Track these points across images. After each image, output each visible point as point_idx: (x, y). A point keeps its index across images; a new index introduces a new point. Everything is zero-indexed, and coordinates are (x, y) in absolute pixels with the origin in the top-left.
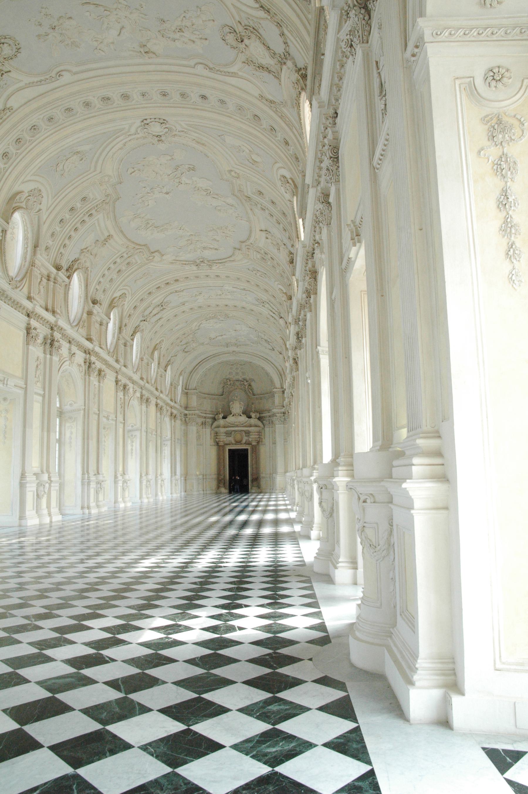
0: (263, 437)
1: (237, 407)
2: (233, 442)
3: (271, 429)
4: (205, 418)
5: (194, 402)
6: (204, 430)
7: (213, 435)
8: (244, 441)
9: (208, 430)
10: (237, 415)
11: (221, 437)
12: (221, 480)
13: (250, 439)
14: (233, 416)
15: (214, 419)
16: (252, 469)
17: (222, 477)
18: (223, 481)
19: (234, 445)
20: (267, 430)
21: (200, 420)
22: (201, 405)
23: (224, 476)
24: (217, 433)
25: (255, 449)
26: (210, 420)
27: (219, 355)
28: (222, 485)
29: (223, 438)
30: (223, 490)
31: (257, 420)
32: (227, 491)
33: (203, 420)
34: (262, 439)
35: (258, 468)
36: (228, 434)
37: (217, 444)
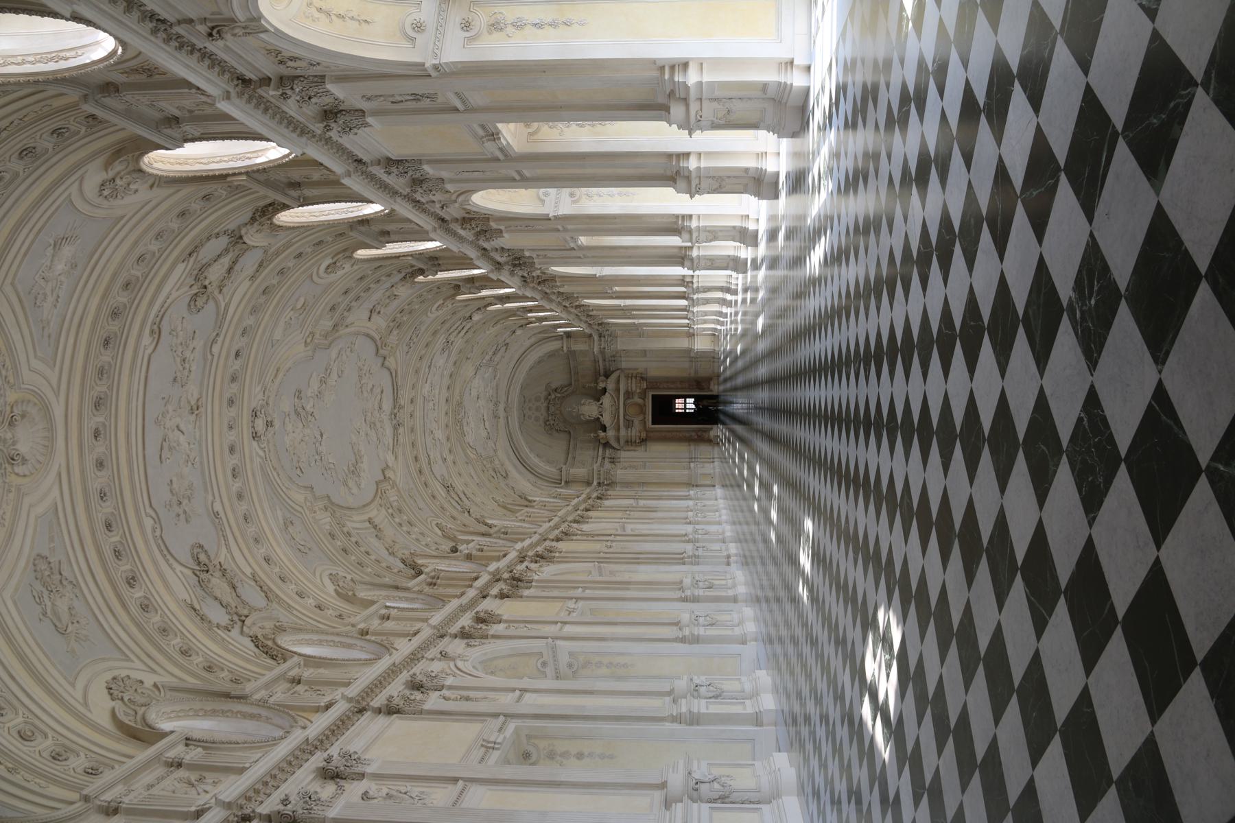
0: (635, 372)
1: (589, 409)
2: (641, 417)
3: (623, 359)
4: (604, 458)
5: (580, 472)
6: (622, 460)
7: (632, 448)
8: (640, 401)
9: (623, 454)
10: (600, 409)
11: (633, 434)
12: (699, 436)
13: (638, 391)
14: (602, 415)
15: (607, 445)
16: (682, 389)
17: (693, 434)
18: (699, 433)
19: (647, 416)
20: (624, 365)
21: (607, 465)
22: (584, 465)
23: (694, 431)
24: (627, 442)
25: (653, 383)
26: (607, 451)
27: (510, 434)
28: (706, 435)
29: (635, 432)
30: (712, 434)
31: (609, 380)
32: (715, 427)
33: (607, 461)
34: (638, 373)
35: (682, 381)
36: (629, 424)
37: (643, 441)
